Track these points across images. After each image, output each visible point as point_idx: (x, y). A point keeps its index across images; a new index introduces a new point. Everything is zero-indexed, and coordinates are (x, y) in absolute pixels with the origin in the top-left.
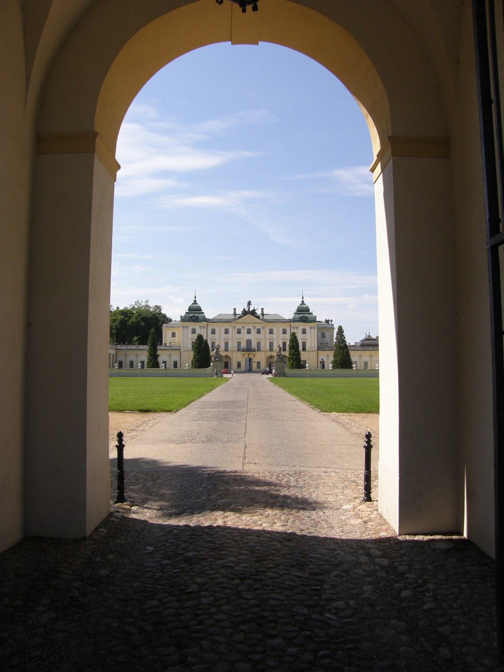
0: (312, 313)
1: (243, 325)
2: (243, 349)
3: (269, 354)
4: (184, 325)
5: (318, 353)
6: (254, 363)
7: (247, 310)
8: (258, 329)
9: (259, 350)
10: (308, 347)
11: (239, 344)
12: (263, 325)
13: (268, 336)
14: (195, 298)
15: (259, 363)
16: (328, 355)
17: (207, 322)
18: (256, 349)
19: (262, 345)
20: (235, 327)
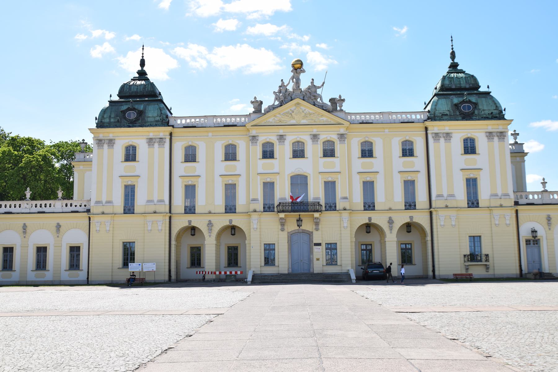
0: (488, 93)
1: (281, 131)
2: (279, 205)
3: (363, 218)
4: (101, 136)
5: (517, 211)
6: (315, 248)
7: (290, 88)
8: (326, 143)
9: (331, 207)
10: (484, 195)
11: (269, 187)
12: (342, 131)
13: (360, 164)
14: (143, 63)
15: (332, 248)
16: (549, 219)
17: (173, 126)
18: (323, 203)
19: (340, 192)
20: (254, 138)
